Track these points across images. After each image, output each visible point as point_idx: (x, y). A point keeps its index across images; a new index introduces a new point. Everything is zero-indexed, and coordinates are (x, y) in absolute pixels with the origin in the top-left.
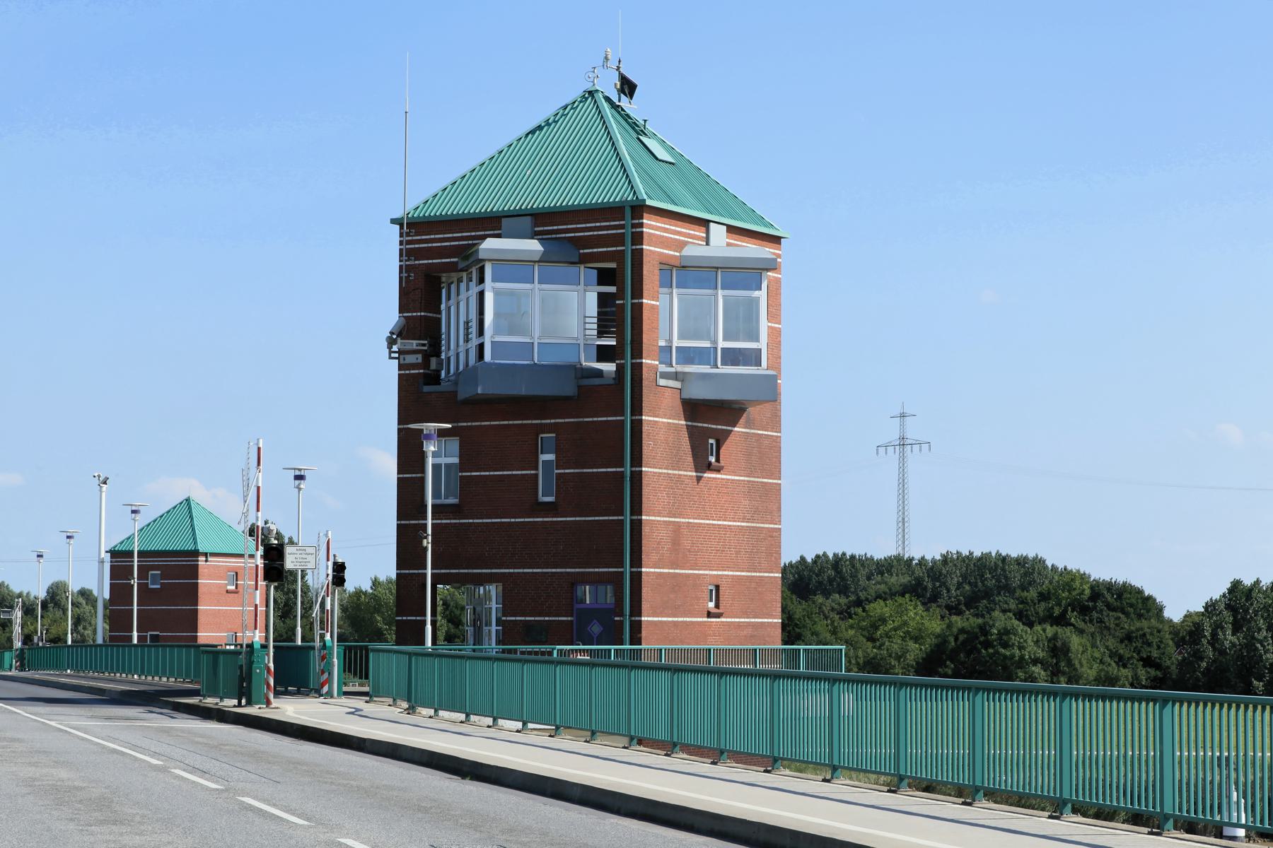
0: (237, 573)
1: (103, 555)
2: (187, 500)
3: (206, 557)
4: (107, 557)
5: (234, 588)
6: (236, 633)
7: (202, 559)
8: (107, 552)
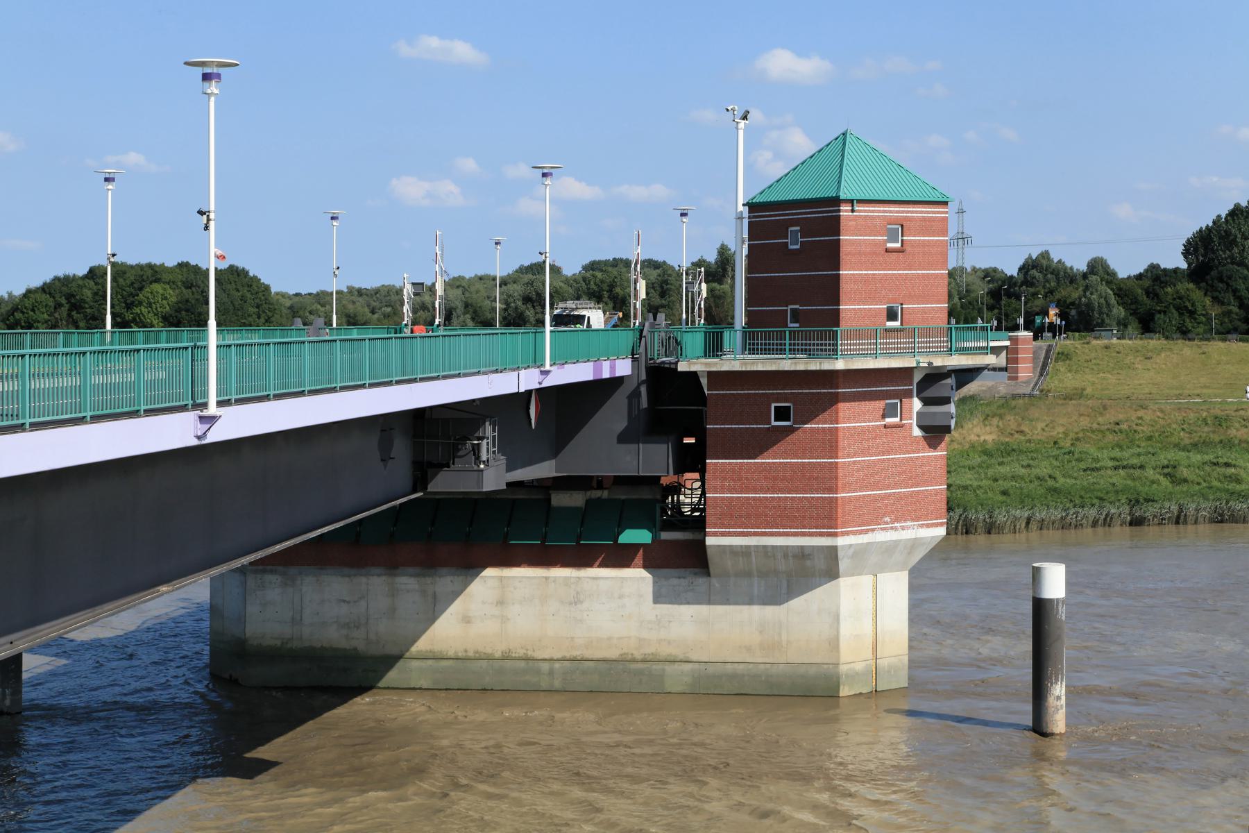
0: (902, 226)
1: (741, 208)
2: (844, 134)
3: (853, 206)
5: (899, 245)
6: (902, 304)
7: (845, 208)
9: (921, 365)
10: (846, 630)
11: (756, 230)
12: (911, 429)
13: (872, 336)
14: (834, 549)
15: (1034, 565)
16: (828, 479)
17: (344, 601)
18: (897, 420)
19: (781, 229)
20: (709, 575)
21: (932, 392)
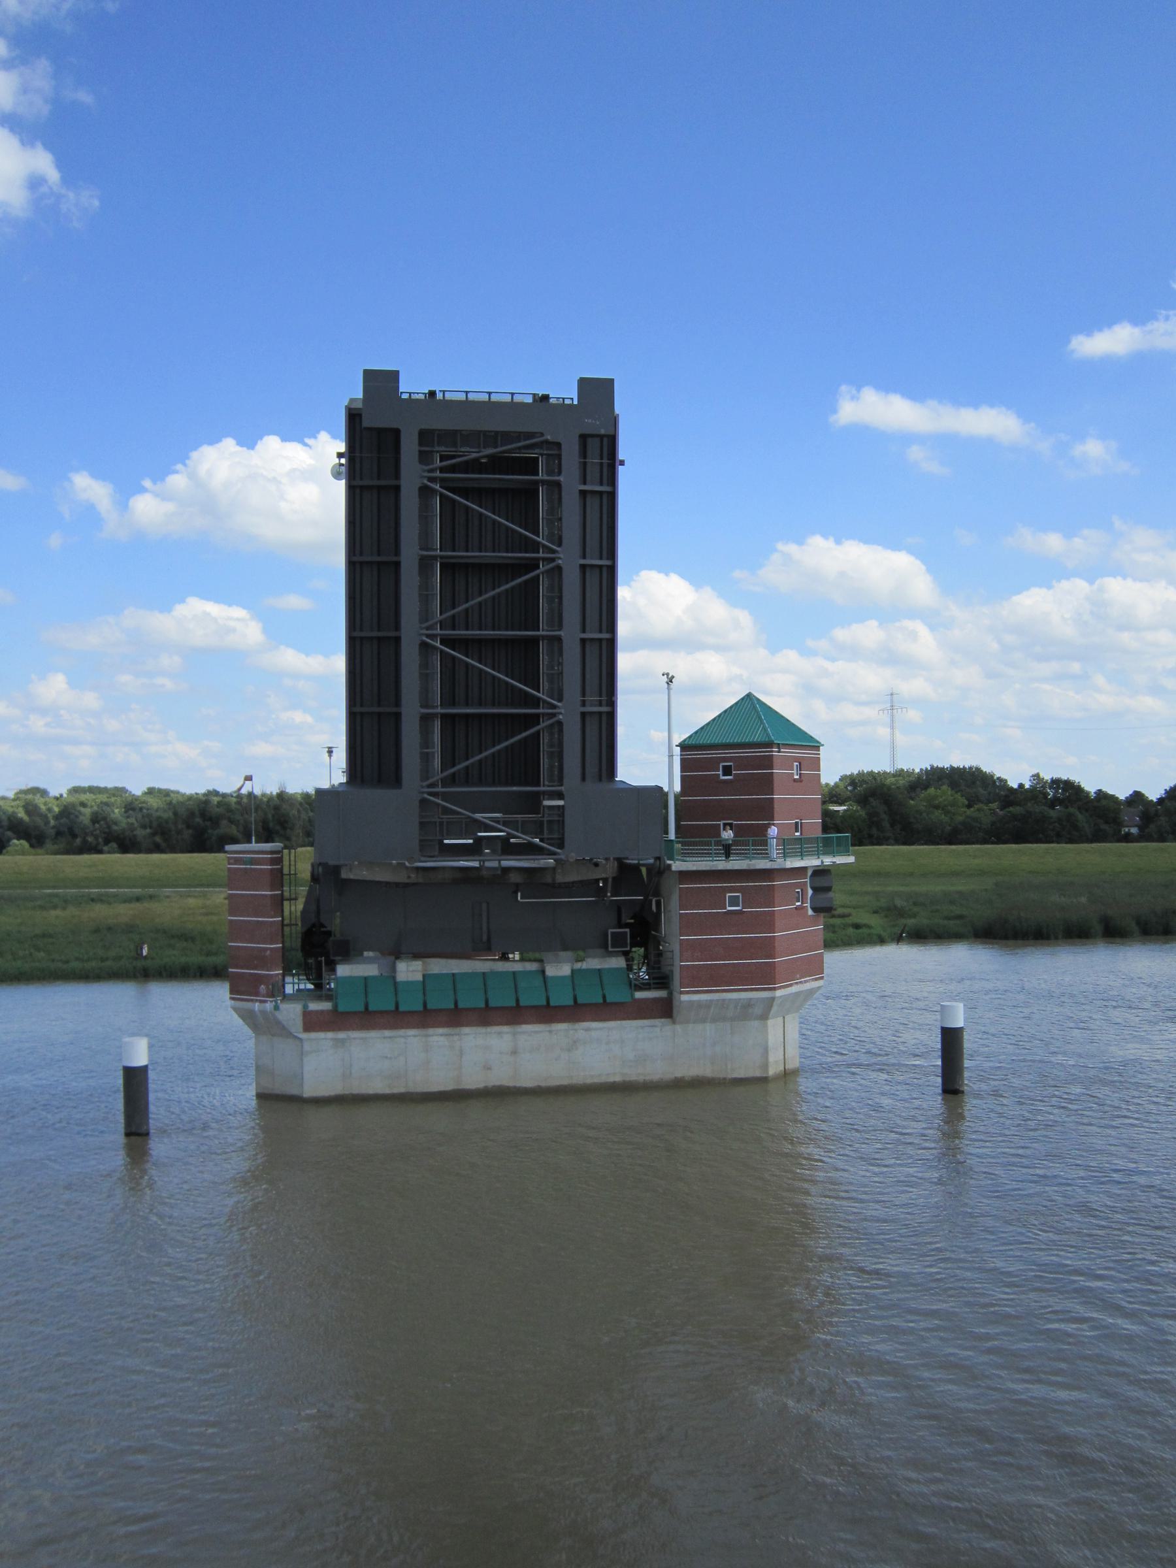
3: (779, 748)
8: (677, 746)
11: (685, 765)
12: (807, 910)
16: (767, 946)
17: (386, 1057)
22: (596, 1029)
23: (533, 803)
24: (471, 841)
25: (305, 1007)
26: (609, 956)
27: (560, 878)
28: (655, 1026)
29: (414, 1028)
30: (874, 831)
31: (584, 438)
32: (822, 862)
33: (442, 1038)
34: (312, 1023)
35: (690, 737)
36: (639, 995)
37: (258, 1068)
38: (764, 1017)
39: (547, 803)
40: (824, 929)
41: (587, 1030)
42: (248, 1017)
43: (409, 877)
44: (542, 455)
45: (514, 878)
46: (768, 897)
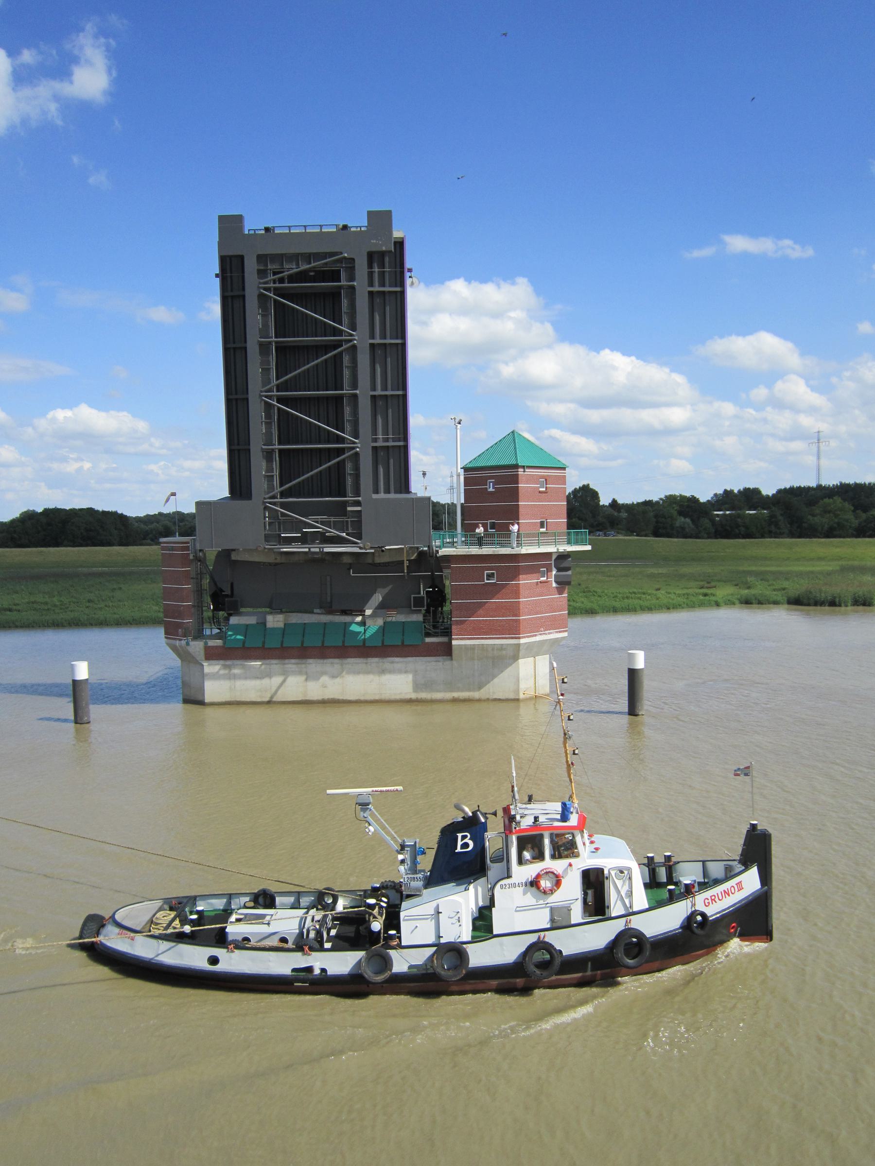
0: (546, 480)
3: (524, 469)
4: (462, 472)
5: (544, 489)
8: (461, 468)
9: (560, 551)
10: (523, 686)
11: (467, 482)
12: (552, 584)
13: (539, 538)
14: (519, 645)
15: (629, 652)
16: (514, 609)
18: (545, 578)
19: (483, 481)
20: (452, 659)
21: (565, 564)
22: (398, 663)
23: (340, 509)
24: (300, 535)
25: (206, 643)
26: (413, 613)
27: (378, 560)
28: (439, 661)
29: (276, 659)
30: (773, 528)
31: (371, 256)
32: (558, 549)
33: (294, 666)
34: (211, 655)
35: (470, 462)
36: (428, 640)
37: (183, 682)
38: (515, 658)
39: (349, 509)
40: (568, 597)
41: (392, 662)
42: (174, 649)
43: (276, 559)
44: (342, 267)
45: (346, 560)
46: (515, 574)
